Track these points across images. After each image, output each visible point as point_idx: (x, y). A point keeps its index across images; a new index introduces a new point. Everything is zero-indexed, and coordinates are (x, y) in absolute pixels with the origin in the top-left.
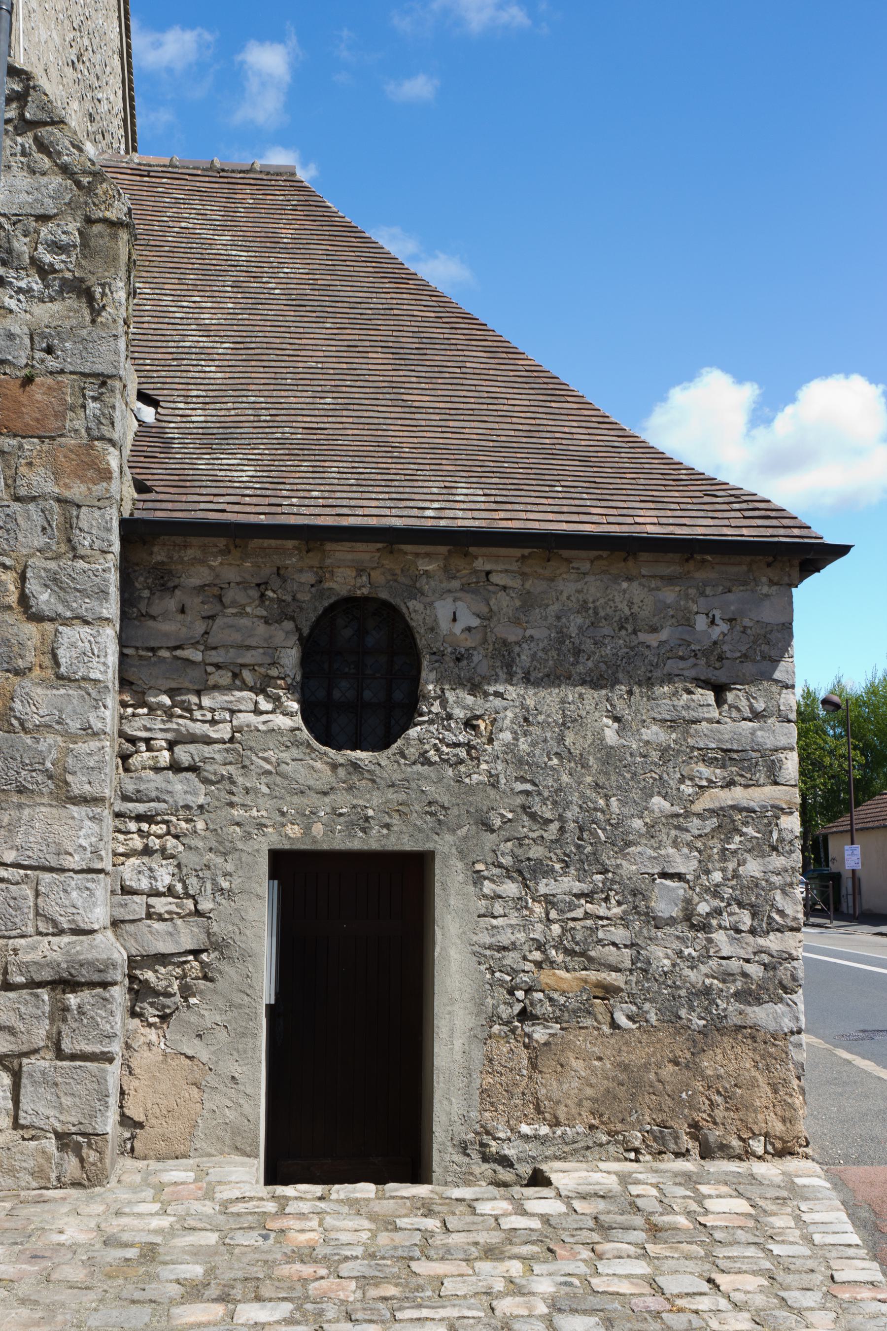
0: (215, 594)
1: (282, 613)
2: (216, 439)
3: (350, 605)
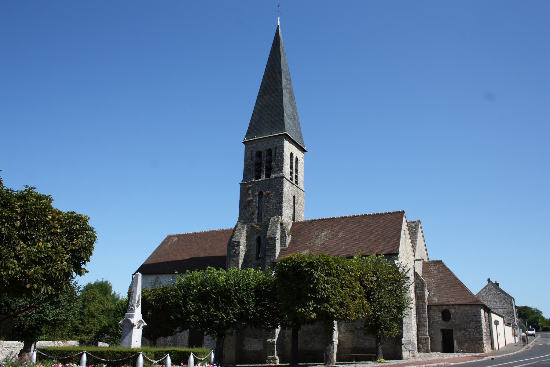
0: (435, 310)
1: (440, 311)
2: (434, 296)
3: (445, 310)
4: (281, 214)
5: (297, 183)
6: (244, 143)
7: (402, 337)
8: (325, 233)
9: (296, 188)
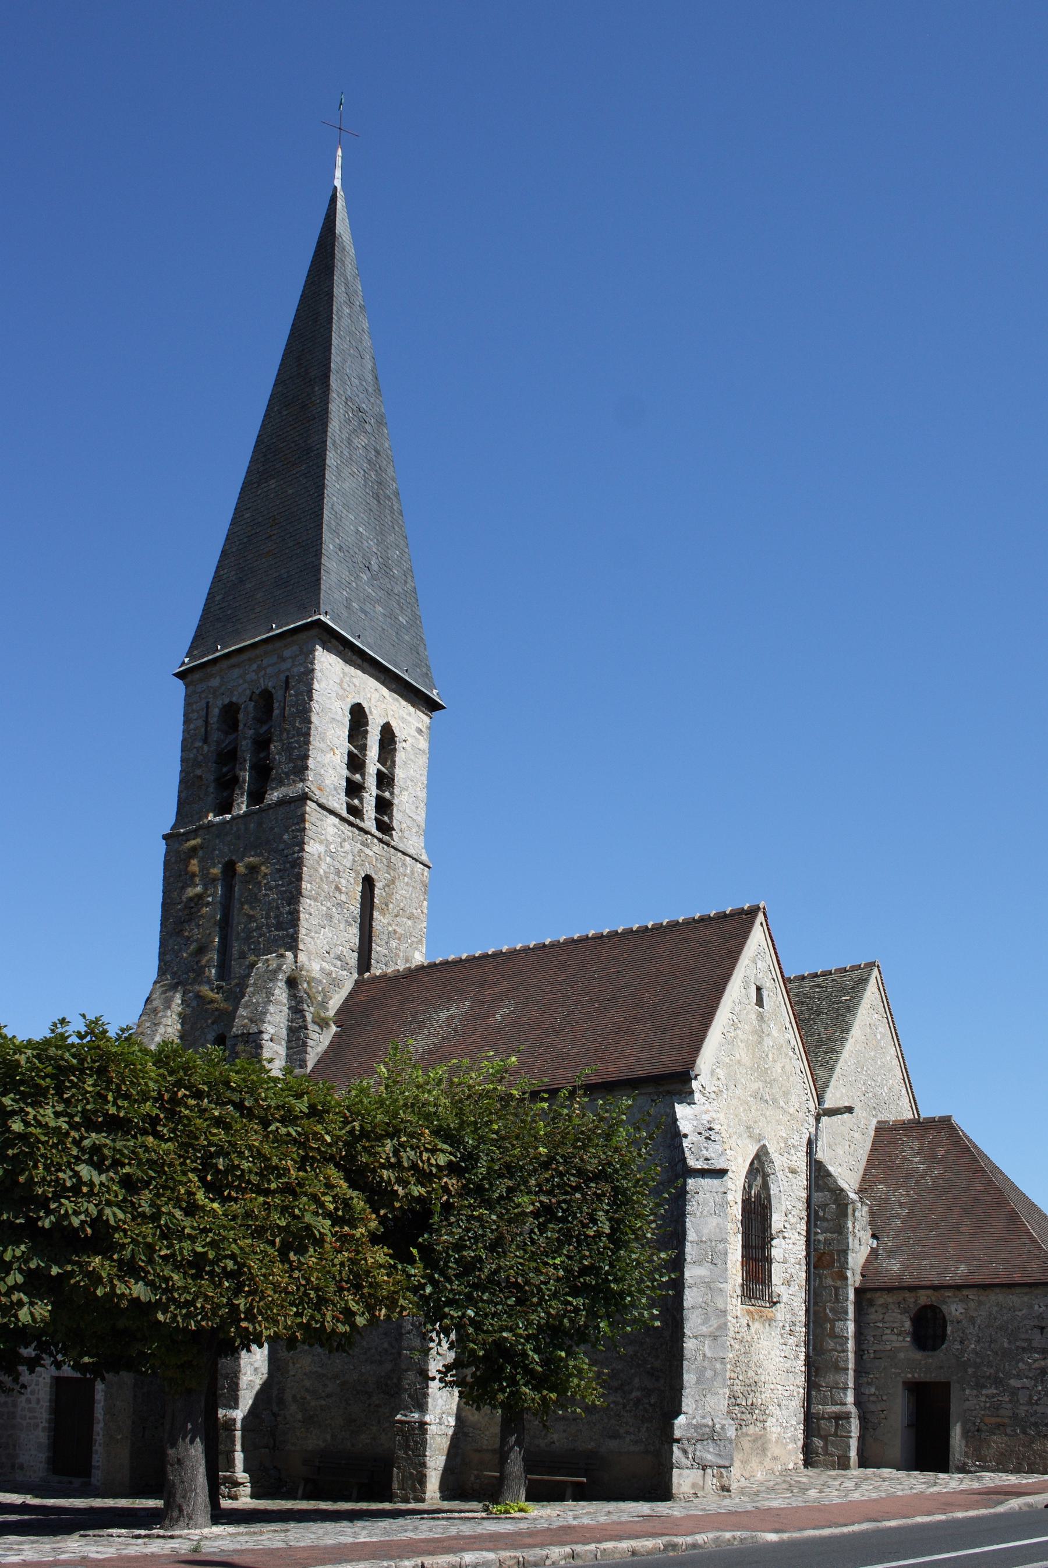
4: (293, 945)
5: (385, 828)
6: (180, 675)
7: (678, 1412)
8: (453, 1011)
9: (378, 847)
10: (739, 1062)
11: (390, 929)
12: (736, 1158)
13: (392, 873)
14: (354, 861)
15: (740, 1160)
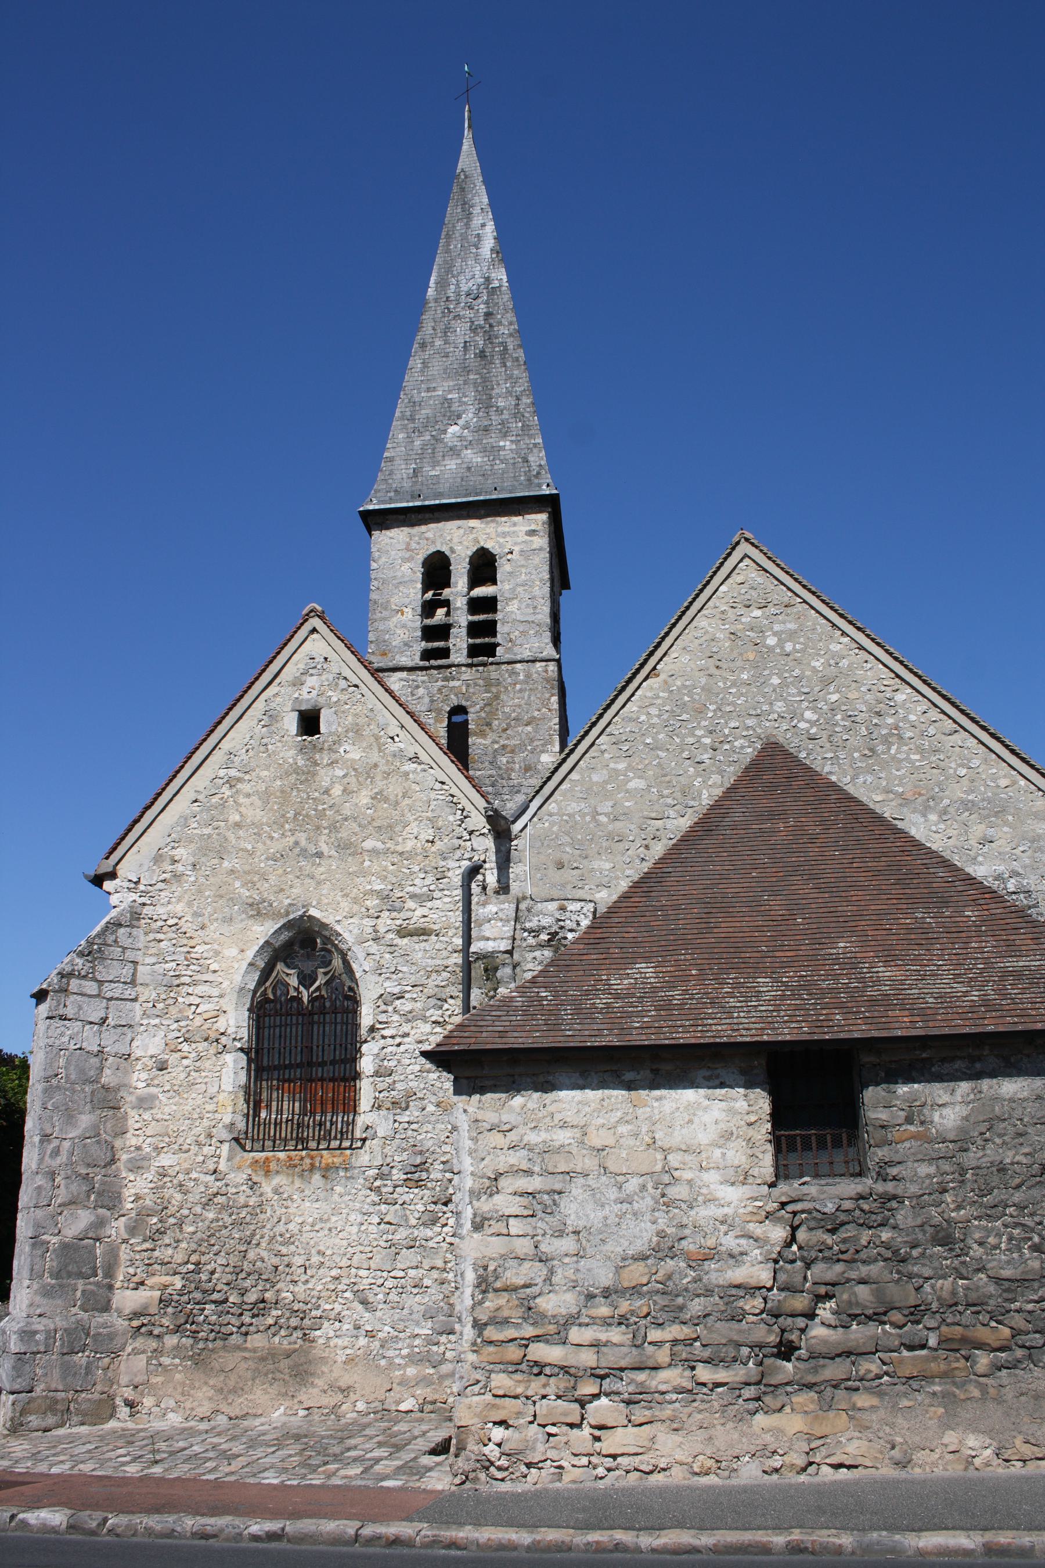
9: (467, 674)
10: (238, 825)
11: (496, 746)
12: (217, 953)
13: (494, 690)
14: (432, 701)
15: (234, 952)
